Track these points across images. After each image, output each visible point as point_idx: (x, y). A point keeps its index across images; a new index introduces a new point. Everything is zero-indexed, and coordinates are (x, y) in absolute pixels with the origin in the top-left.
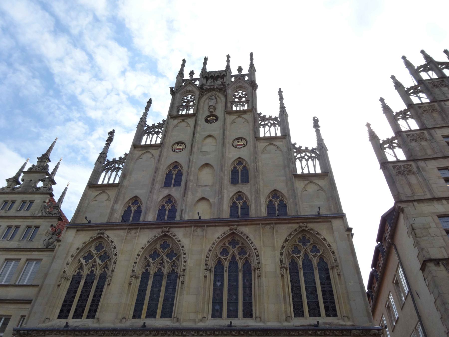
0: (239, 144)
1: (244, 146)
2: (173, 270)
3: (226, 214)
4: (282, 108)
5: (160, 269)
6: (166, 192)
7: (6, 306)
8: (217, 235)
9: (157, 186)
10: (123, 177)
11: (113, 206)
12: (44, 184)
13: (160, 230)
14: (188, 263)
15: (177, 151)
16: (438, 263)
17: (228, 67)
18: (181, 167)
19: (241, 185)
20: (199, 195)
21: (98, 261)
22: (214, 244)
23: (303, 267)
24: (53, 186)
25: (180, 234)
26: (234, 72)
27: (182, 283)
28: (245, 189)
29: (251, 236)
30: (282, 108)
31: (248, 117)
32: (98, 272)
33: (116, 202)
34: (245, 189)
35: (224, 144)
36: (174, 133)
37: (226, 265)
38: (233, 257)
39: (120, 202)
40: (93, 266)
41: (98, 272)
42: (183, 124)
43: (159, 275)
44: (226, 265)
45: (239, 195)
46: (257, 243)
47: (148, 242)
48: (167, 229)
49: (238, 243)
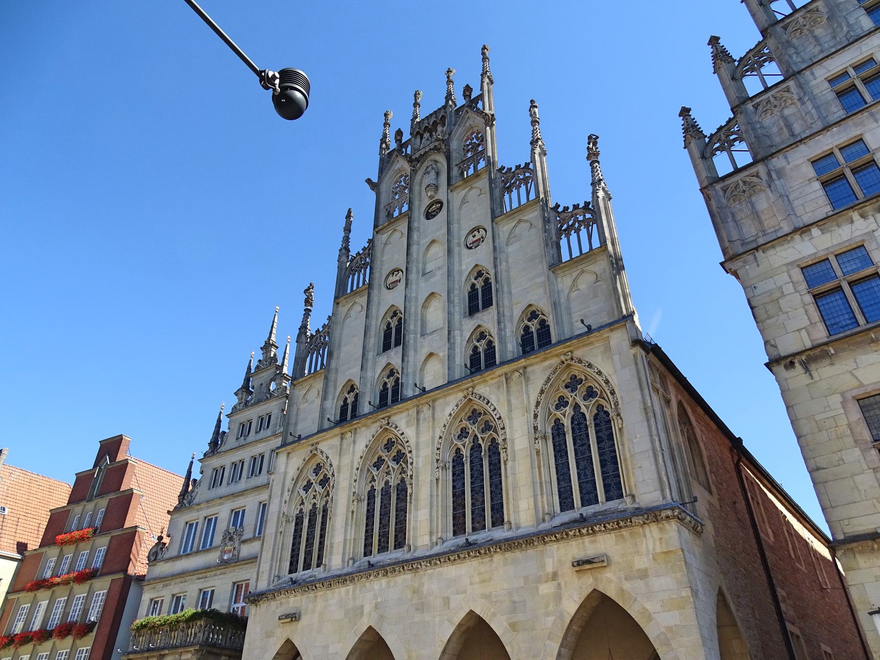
6: (383, 361)
9: (370, 355)
11: (322, 405)
12: (277, 384)
13: (378, 424)
16: (792, 364)
22: (445, 426)
23: (573, 428)
29: (493, 399)
32: (320, 505)
33: (324, 398)
36: (385, 258)
39: (330, 397)
40: (314, 497)
47: (367, 446)
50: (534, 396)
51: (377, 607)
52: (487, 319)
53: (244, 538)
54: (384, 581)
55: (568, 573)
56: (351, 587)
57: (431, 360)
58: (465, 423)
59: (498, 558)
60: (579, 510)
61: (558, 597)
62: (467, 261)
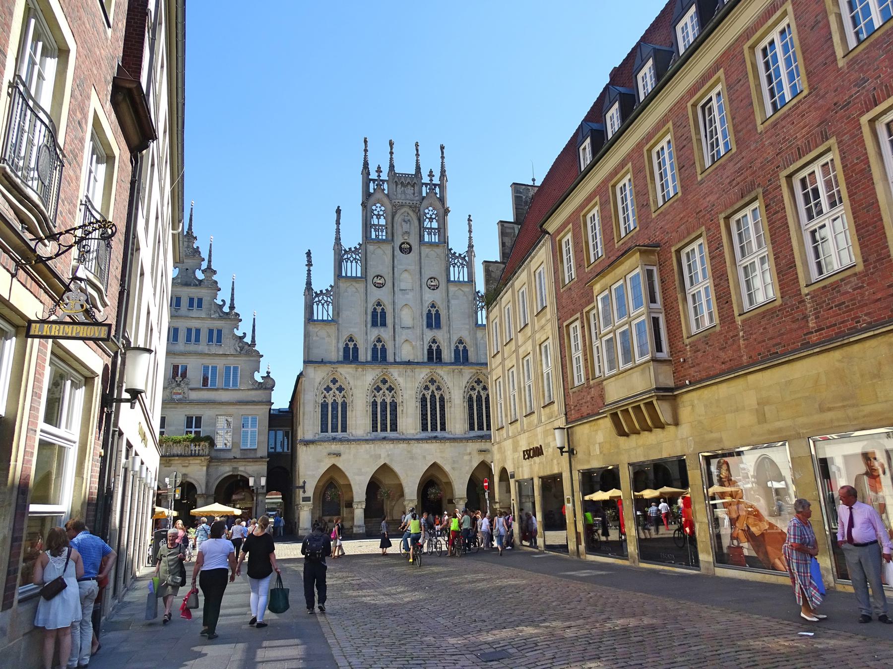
4: (471, 246)
5: (384, 400)
7: (224, 407)
8: (422, 375)
10: (337, 312)
14: (405, 397)
17: (418, 168)
19: (435, 331)
20: (404, 337)
21: (337, 392)
24: (215, 278)
26: (426, 179)
29: (445, 377)
30: (471, 246)
31: (440, 250)
32: (340, 401)
33: (338, 342)
37: (428, 397)
38: (433, 392)
41: (340, 401)
42: (379, 251)
43: (384, 404)
44: (428, 397)
46: (450, 385)
50: (465, 383)
51: (388, 455)
52: (441, 335)
53: (190, 386)
54: (392, 446)
55: (475, 453)
56: (372, 446)
57: (409, 344)
58: (428, 383)
59: (448, 444)
60: (476, 432)
61: (471, 461)
62: (429, 296)
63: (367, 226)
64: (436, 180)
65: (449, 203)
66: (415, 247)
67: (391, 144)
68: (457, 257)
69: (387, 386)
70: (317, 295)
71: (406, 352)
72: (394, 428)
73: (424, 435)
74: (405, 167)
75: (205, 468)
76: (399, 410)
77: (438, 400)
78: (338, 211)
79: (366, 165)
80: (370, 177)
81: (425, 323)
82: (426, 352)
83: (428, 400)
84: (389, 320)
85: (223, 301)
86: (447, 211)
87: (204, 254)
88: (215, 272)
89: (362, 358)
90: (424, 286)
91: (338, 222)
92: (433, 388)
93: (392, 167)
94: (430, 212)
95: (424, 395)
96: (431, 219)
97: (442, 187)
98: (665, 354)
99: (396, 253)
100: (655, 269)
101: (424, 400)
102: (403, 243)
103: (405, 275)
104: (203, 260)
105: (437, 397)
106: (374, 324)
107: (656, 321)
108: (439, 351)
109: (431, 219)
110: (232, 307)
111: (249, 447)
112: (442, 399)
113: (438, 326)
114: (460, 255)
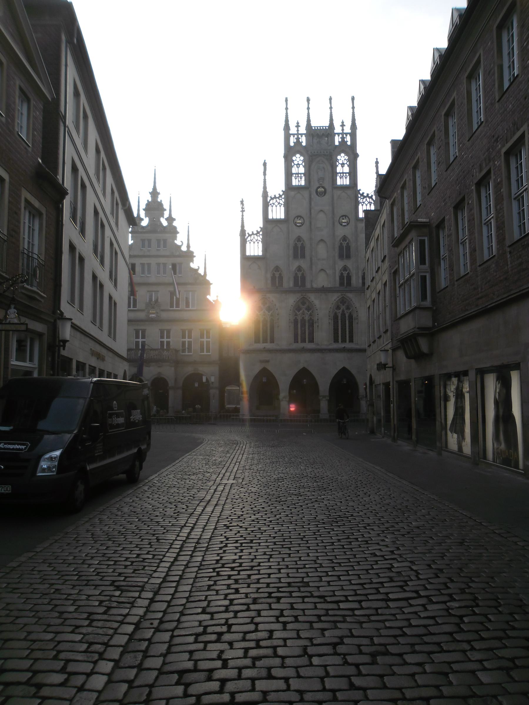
0: (343, 221)
1: (348, 224)
2: (311, 318)
3: (338, 285)
5: (303, 318)
6: (296, 264)
15: (298, 225)
18: (303, 241)
25: (312, 297)
26: (338, 129)
27: (318, 326)
28: (349, 264)
34: (349, 264)
35: (334, 224)
37: (340, 316)
43: (303, 320)
45: (345, 268)
48: (304, 294)
49: (345, 302)
62: (340, 232)
63: (289, 175)
64: (347, 130)
65: (359, 151)
66: (329, 189)
67: (308, 100)
68: (364, 197)
69: (305, 306)
70: (249, 235)
71: (322, 281)
72: (311, 340)
73: (335, 346)
74: (320, 121)
75: (173, 369)
76: (315, 325)
77: (347, 318)
78: (265, 164)
79: (287, 121)
80: (291, 132)
81: (337, 254)
82: (338, 278)
83: (339, 318)
84: (307, 253)
85: (182, 242)
86: (356, 156)
87: (166, 206)
88: (174, 220)
89: (285, 285)
90: (337, 223)
91: (265, 174)
92: (343, 307)
93: (309, 121)
94: (342, 158)
95: (336, 314)
96: (343, 165)
97: (353, 134)
98: (428, 303)
99: (312, 196)
100: (426, 239)
101: (335, 317)
102: (319, 187)
103: (321, 215)
104: (165, 210)
105: (347, 315)
106: (295, 257)
107: (424, 278)
108: (349, 278)
109: (343, 165)
110: (188, 246)
111: (205, 353)
112: (351, 317)
113: (348, 257)
114: (368, 194)
